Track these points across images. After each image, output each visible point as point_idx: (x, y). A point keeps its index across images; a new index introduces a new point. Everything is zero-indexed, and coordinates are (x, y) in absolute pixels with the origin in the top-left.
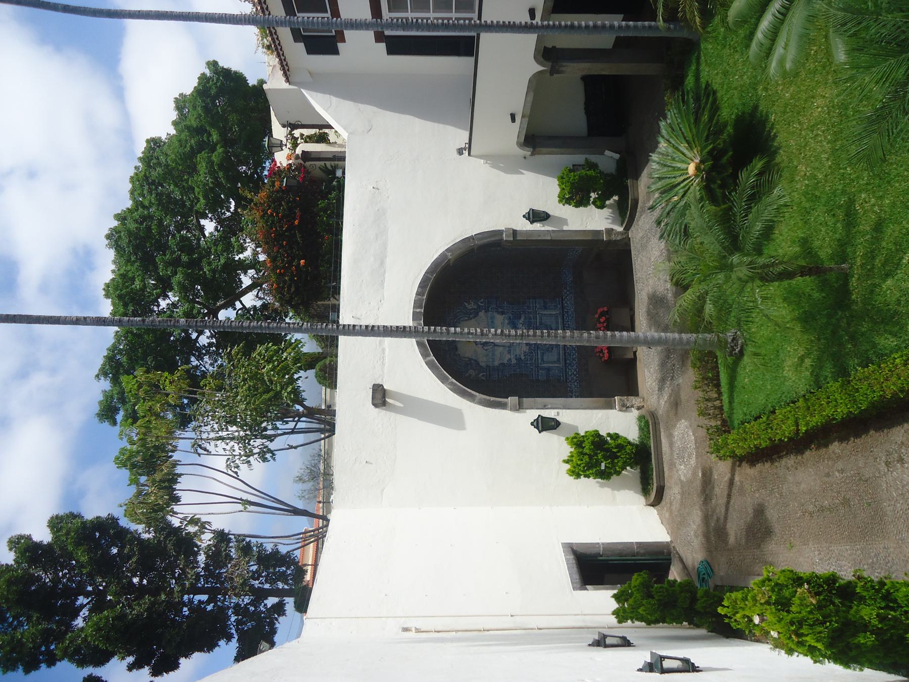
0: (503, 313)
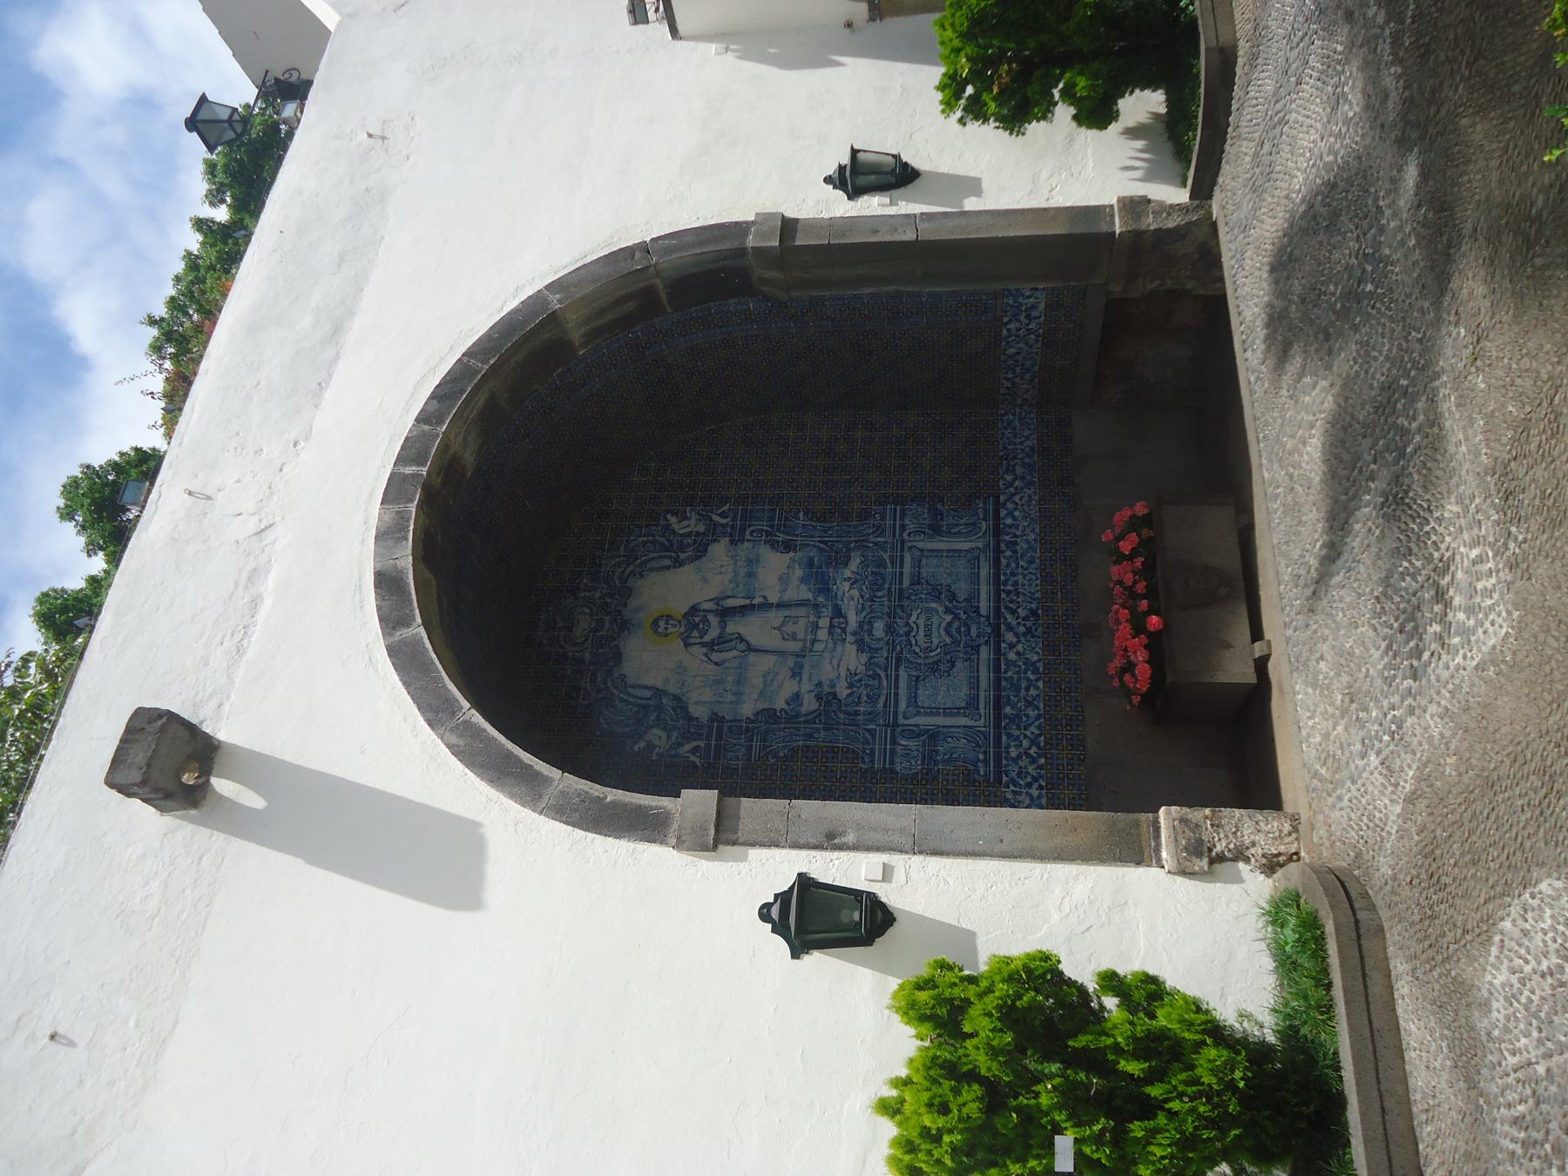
0: (788, 547)
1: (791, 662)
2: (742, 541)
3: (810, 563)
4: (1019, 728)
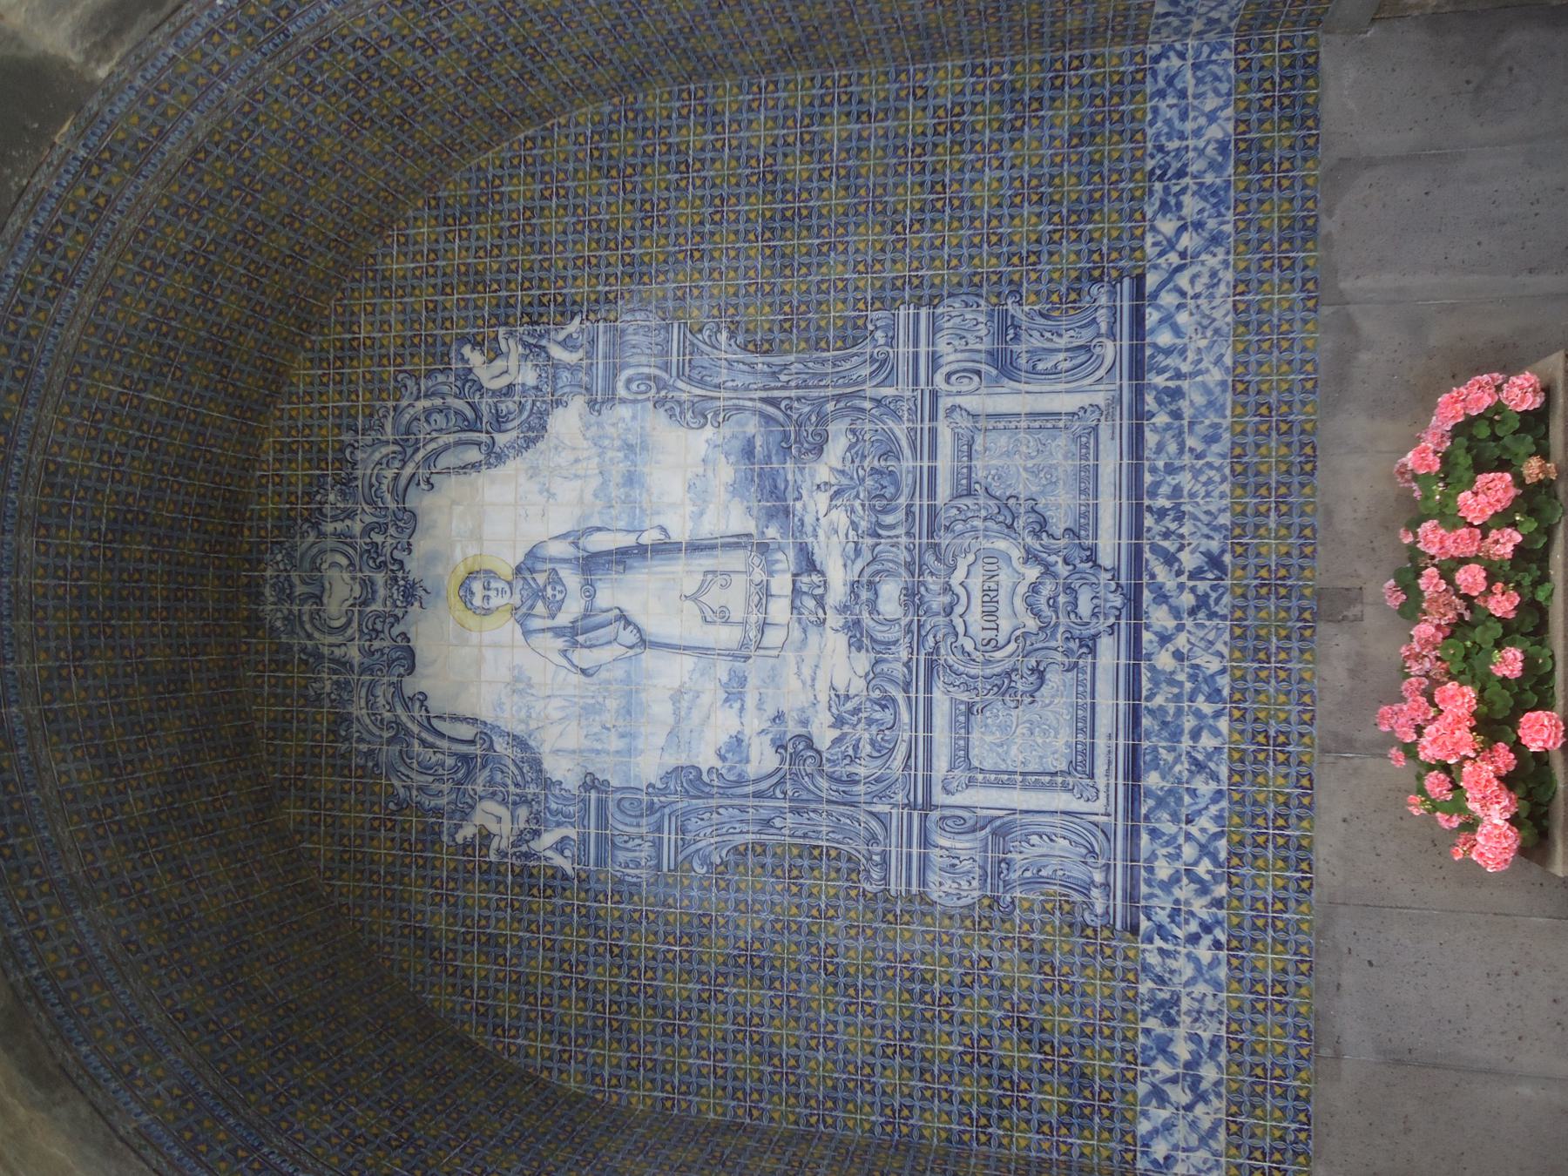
0: (700, 414)
1: (722, 669)
2: (611, 399)
3: (748, 452)
4: (1175, 818)
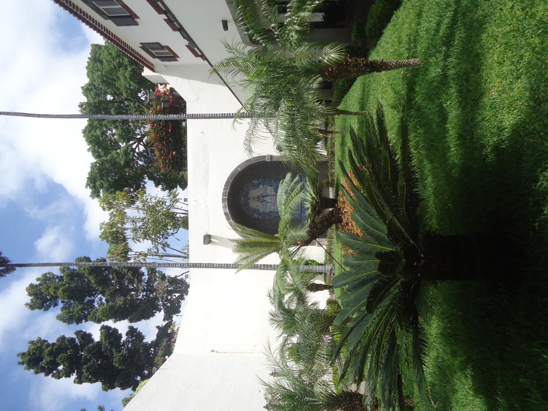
0: (271, 186)
